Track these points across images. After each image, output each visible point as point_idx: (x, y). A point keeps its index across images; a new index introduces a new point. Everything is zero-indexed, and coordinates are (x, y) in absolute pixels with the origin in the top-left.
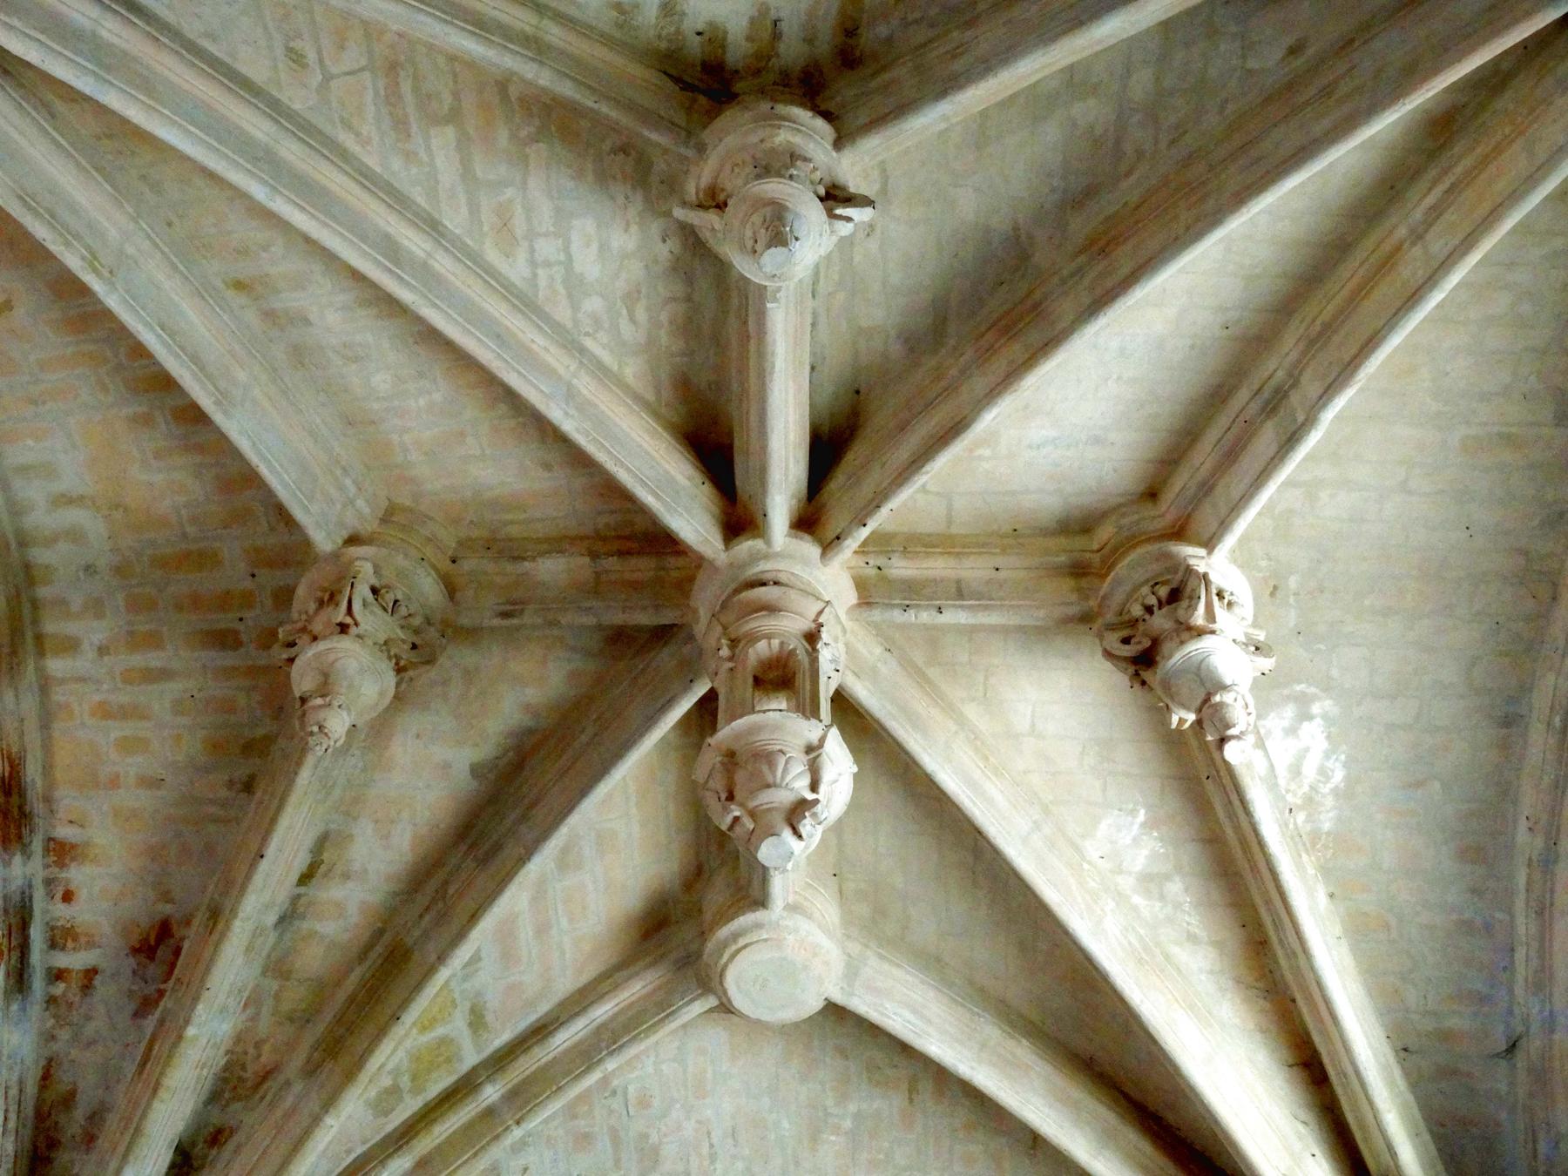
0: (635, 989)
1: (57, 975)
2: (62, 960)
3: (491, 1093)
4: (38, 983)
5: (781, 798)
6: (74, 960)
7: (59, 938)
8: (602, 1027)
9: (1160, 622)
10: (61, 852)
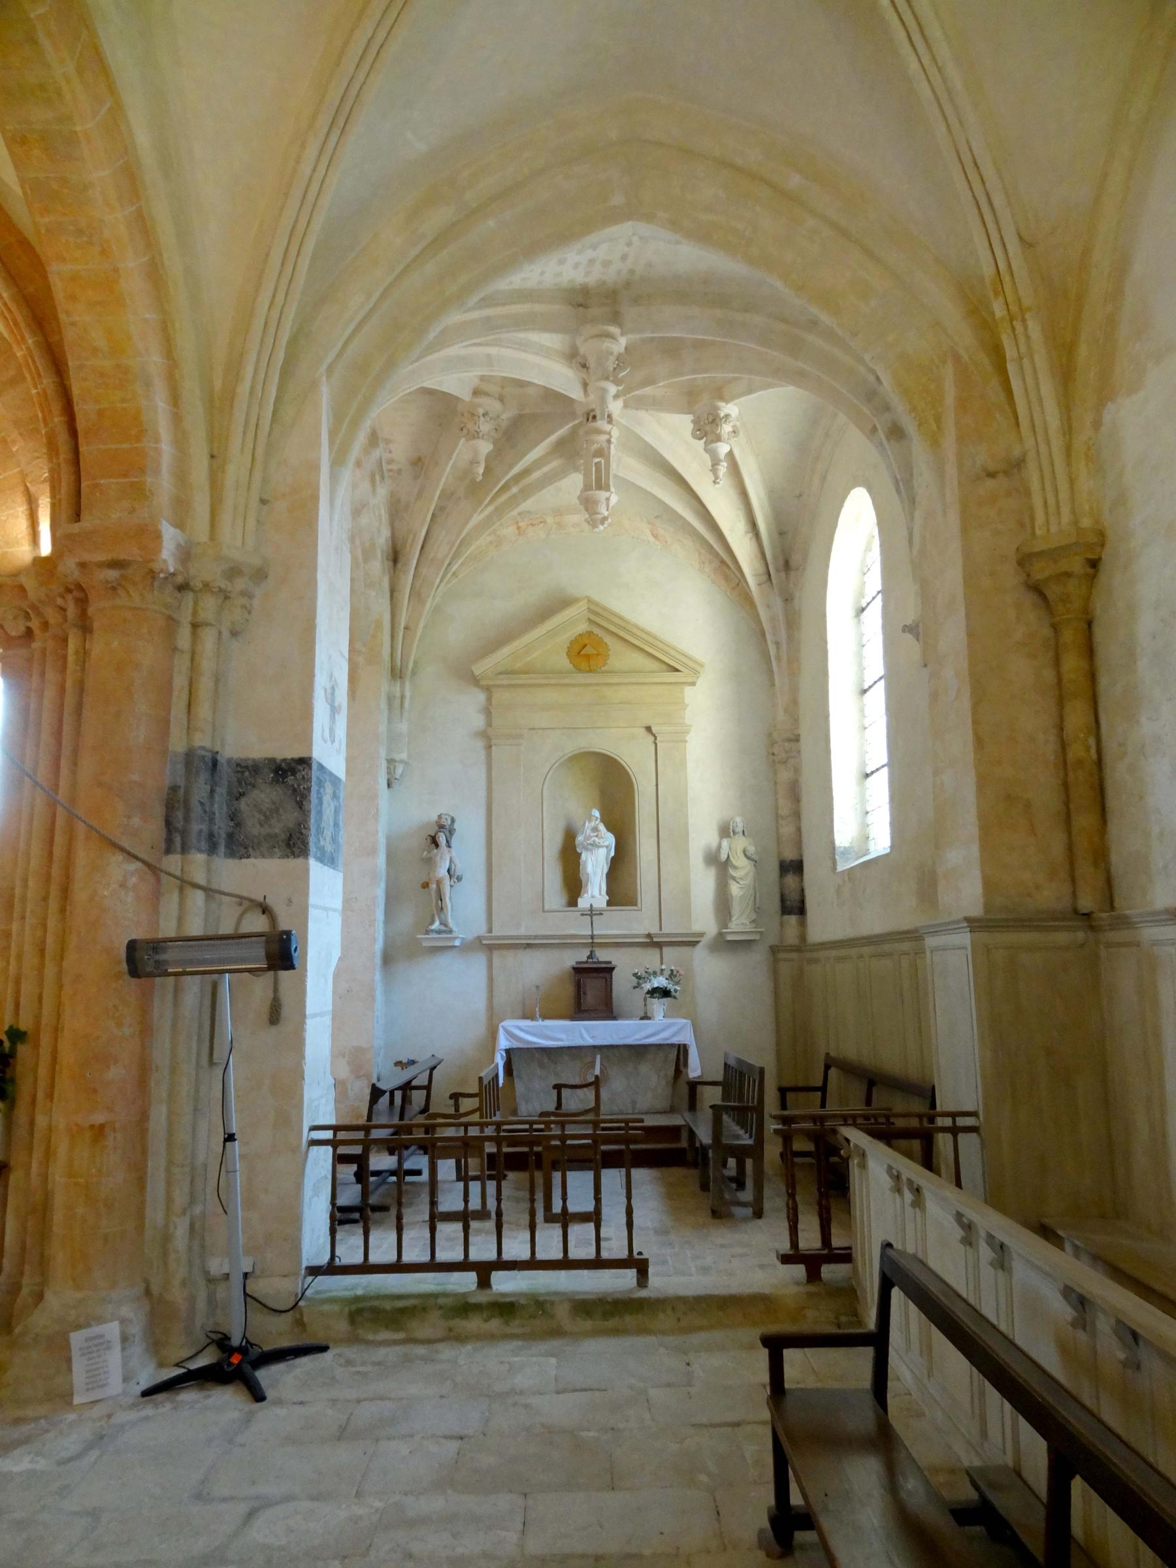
0: (555, 463)
1: (391, 470)
2: (390, 467)
3: (515, 490)
4: (386, 474)
5: (600, 516)
6: (394, 467)
7: (390, 462)
8: (545, 474)
9: (708, 428)
10: (388, 442)
